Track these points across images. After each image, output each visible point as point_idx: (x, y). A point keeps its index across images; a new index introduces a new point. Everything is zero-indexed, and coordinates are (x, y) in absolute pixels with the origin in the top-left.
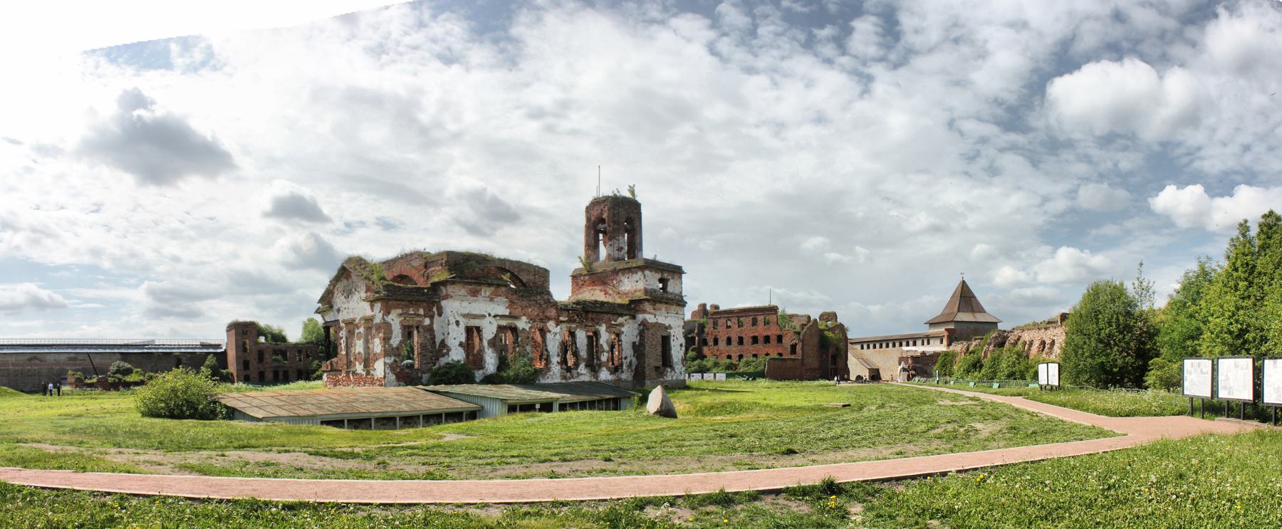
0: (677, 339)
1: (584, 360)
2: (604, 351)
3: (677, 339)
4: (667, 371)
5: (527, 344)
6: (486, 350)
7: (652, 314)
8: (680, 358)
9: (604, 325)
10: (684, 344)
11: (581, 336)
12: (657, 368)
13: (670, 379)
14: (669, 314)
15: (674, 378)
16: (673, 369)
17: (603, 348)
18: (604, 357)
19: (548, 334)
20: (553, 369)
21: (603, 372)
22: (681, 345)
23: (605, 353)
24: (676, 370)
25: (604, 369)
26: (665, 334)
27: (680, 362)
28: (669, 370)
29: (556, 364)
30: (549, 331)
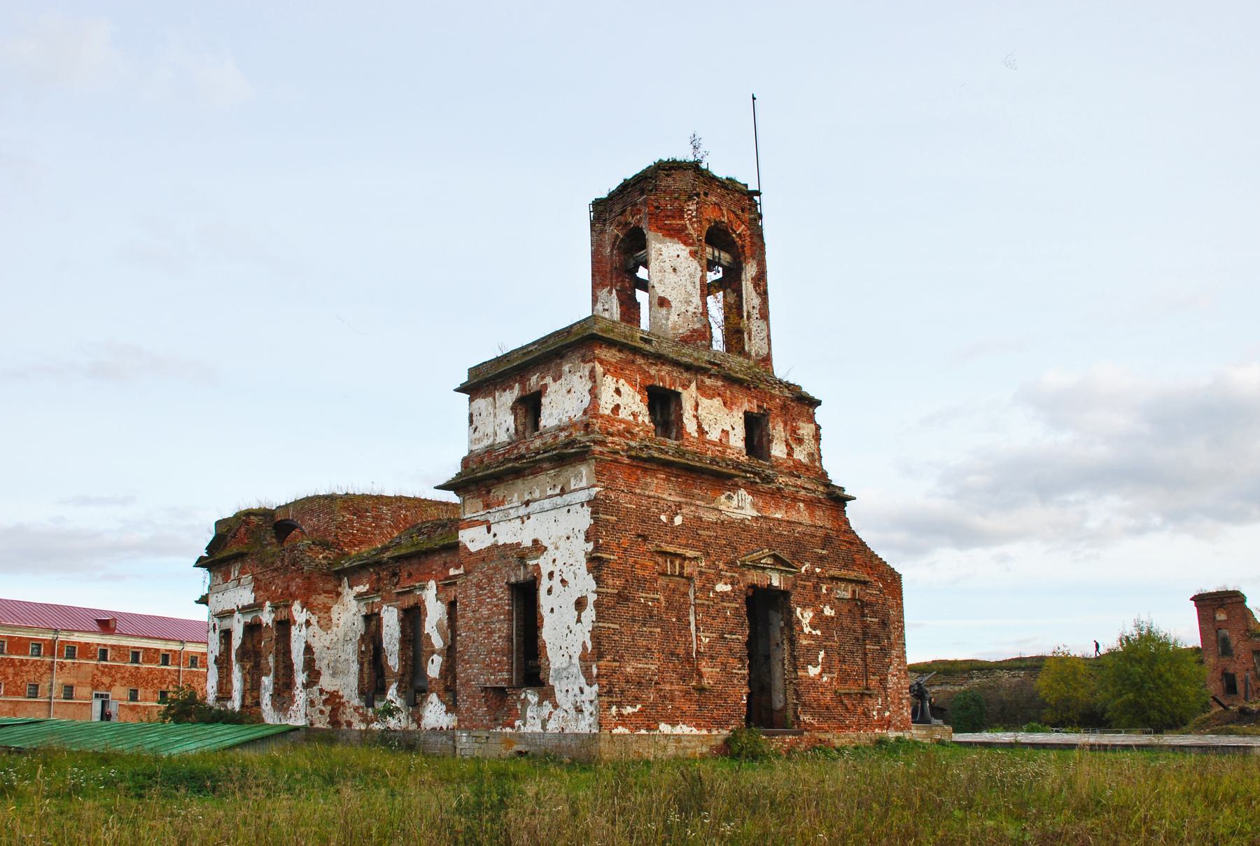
0: (563, 581)
1: (395, 675)
2: (433, 652)
3: (563, 581)
4: (525, 703)
5: (271, 652)
6: (234, 667)
7: (482, 523)
8: (577, 651)
9: (432, 584)
10: (592, 598)
11: (390, 618)
12: (500, 693)
13: (538, 729)
14: (533, 506)
15: (552, 726)
16: (547, 694)
17: (432, 645)
18: (434, 669)
19: (293, 627)
20: (297, 698)
21: (430, 707)
22: (580, 604)
23: (435, 657)
24: (559, 696)
25: (433, 697)
26: (520, 576)
27: (576, 669)
28: (533, 698)
29: (301, 688)
30: (295, 623)
